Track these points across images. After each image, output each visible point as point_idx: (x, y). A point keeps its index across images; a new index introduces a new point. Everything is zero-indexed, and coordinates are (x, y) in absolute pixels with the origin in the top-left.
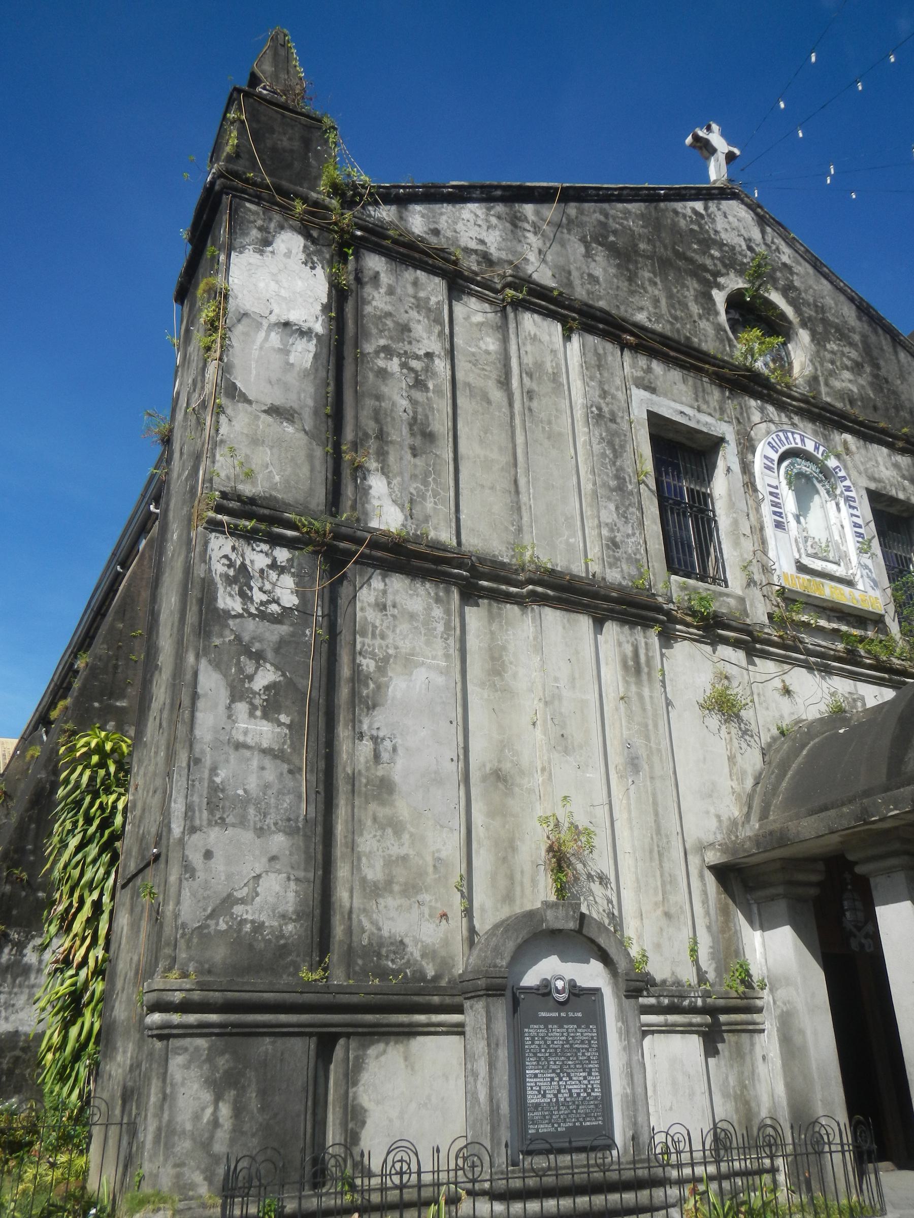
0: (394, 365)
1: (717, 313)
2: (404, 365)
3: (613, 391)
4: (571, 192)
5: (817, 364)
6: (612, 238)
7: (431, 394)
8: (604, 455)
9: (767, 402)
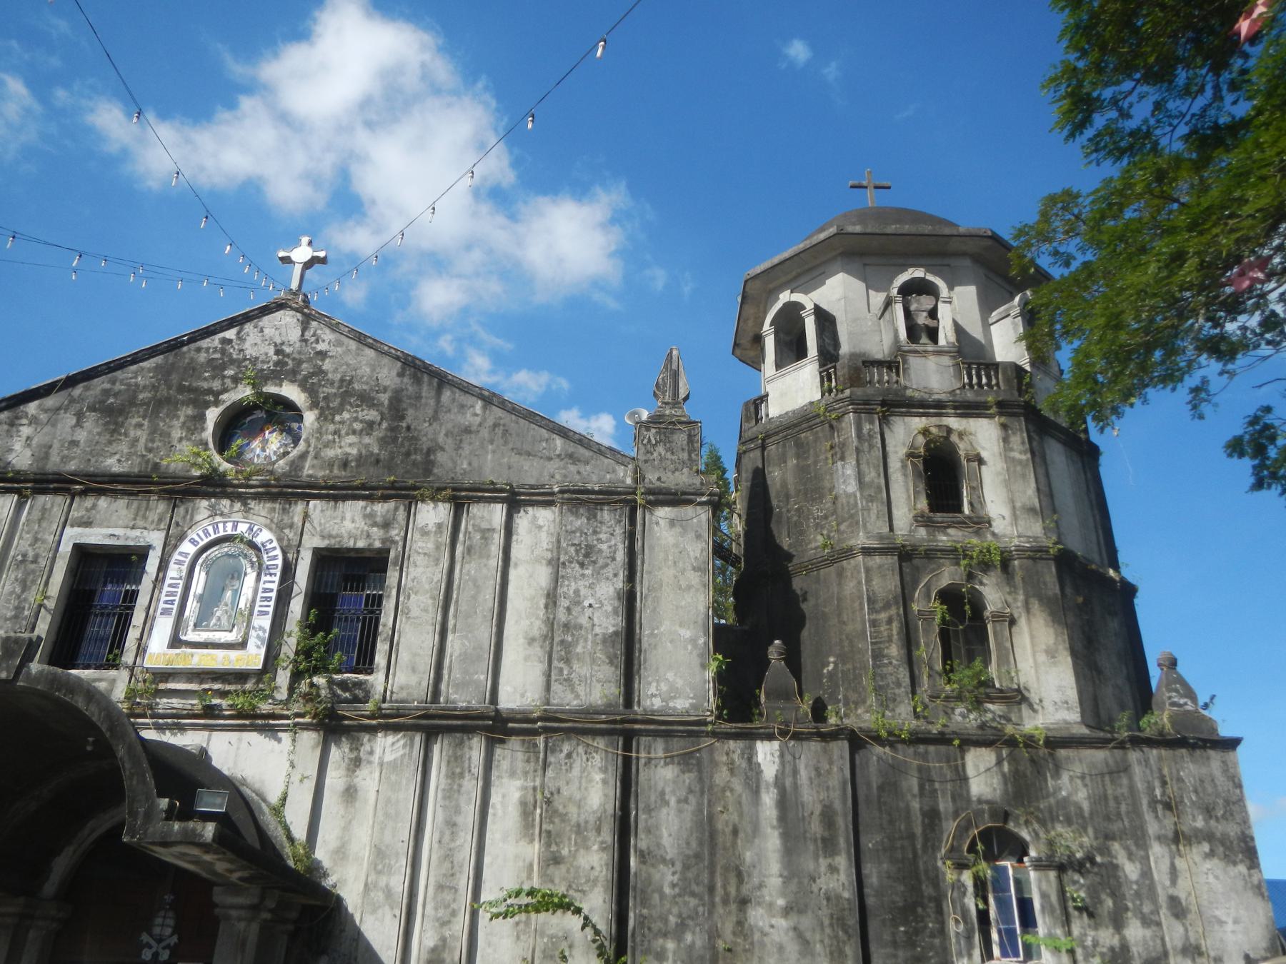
1: (203, 429)
3: (46, 537)
4: (78, 377)
6: (111, 400)
8: (13, 592)
9: (222, 498)
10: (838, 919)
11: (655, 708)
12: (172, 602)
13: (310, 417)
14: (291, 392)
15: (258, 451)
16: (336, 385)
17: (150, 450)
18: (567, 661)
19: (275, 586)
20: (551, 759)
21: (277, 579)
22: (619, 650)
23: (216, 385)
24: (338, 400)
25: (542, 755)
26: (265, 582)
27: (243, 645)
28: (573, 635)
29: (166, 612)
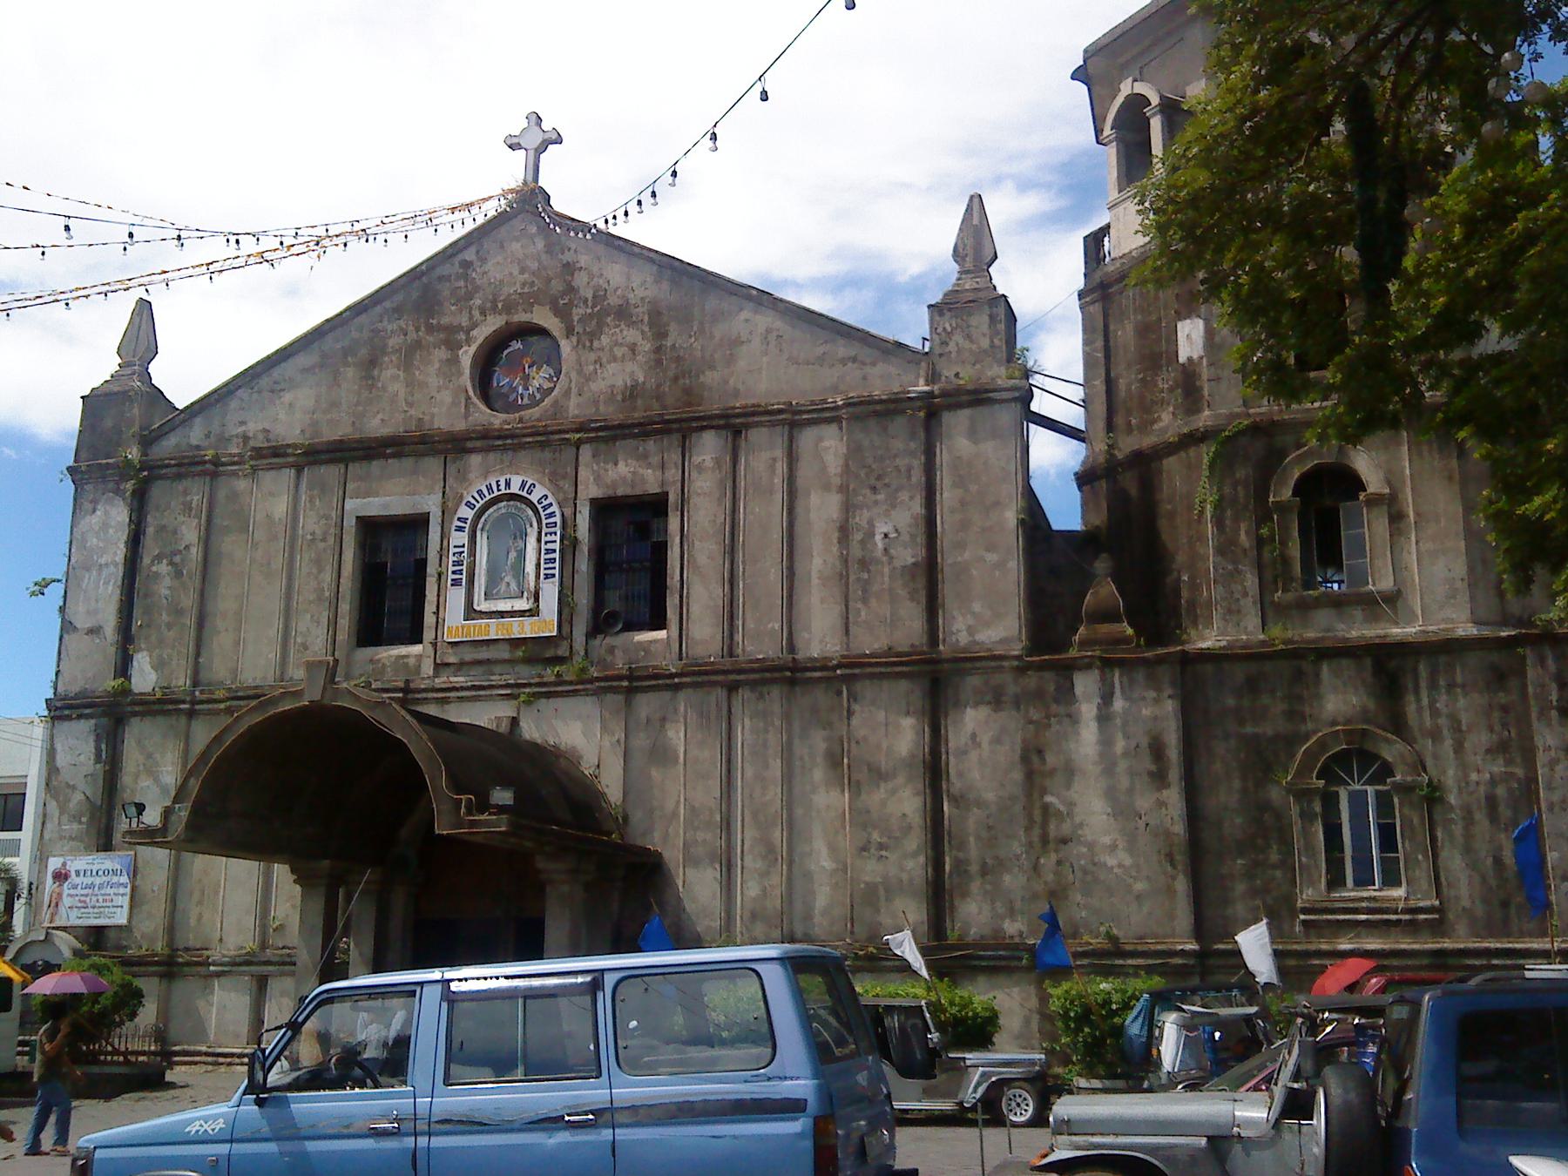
0: (163, 568)
1: (460, 374)
2: (171, 563)
5: (574, 375)
7: (184, 579)
10: (1167, 855)
11: (962, 644)
12: (460, 572)
13: (566, 347)
14: (543, 317)
15: (520, 390)
16: (590, 304)
17: (410, 405)
18: (865, 601)
19: (557, 546)
20: (856, 707)
21: (558, 538)
22: (921, 583)
23: (464, 321)
24: (594, 322)
25: (845, 705)
26: (546, 543)
27: (533, 612)
28: (869, 572)
29: (456, 583)
